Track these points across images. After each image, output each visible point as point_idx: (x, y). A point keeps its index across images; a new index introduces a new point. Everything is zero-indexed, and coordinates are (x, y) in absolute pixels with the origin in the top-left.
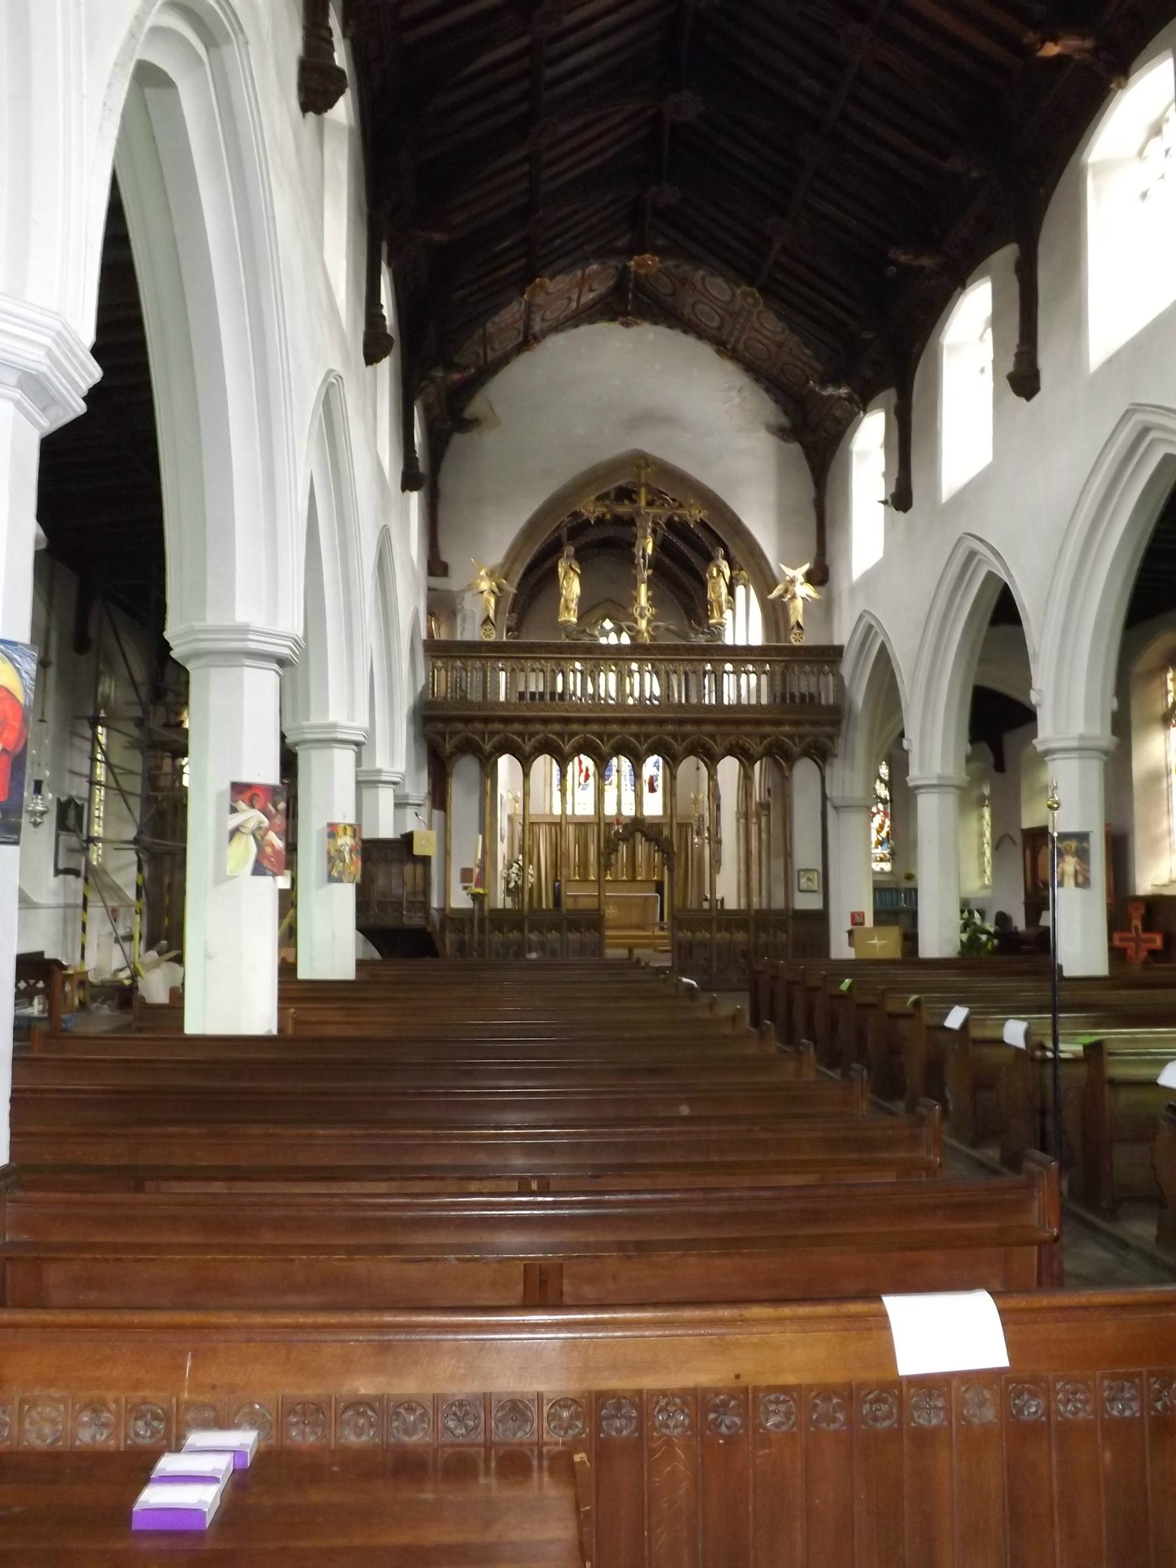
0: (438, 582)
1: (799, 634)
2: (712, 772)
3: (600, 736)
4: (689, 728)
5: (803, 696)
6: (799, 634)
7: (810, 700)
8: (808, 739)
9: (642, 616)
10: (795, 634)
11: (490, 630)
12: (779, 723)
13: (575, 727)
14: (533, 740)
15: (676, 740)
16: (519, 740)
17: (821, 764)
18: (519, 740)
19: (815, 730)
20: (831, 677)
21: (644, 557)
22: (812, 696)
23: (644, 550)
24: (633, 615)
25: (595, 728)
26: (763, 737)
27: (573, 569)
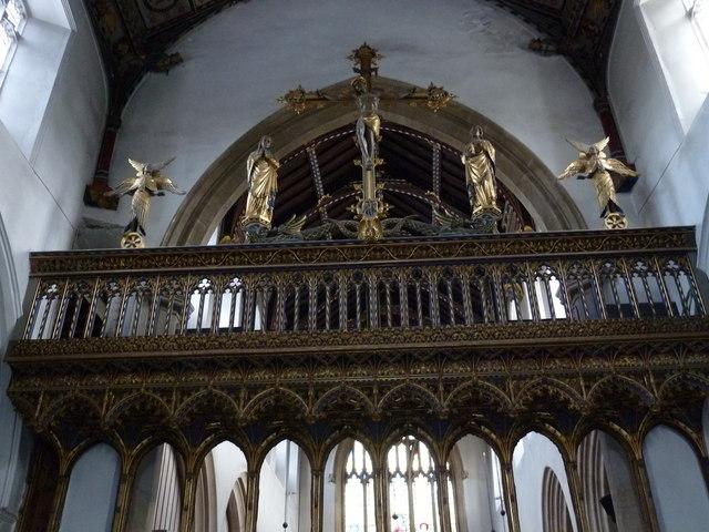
0: (102, 216)
1: (618, 218)
2: (506, 460)
3: (302, 389)
4: (455, 370)
5: (641, 306)
6: (618, 218)
7: (656, 311)
8: (670, 378)
9: (369, 212)
10: (611, 218)
11: (137, 237)
12: (609, 351)
13: (260, 376)
14: (187, 400)
15: (436, 391)
16: (163, 401)
17: (694, 436)
18: (163, 401)
19: (680, 361)
20: (683, 278)
21: (367, 136)
22: (661, 307)
23: (368, 128)
24: (355, 213)
25: (293, 375)
26: (590, 377)
27: (267, 160)
